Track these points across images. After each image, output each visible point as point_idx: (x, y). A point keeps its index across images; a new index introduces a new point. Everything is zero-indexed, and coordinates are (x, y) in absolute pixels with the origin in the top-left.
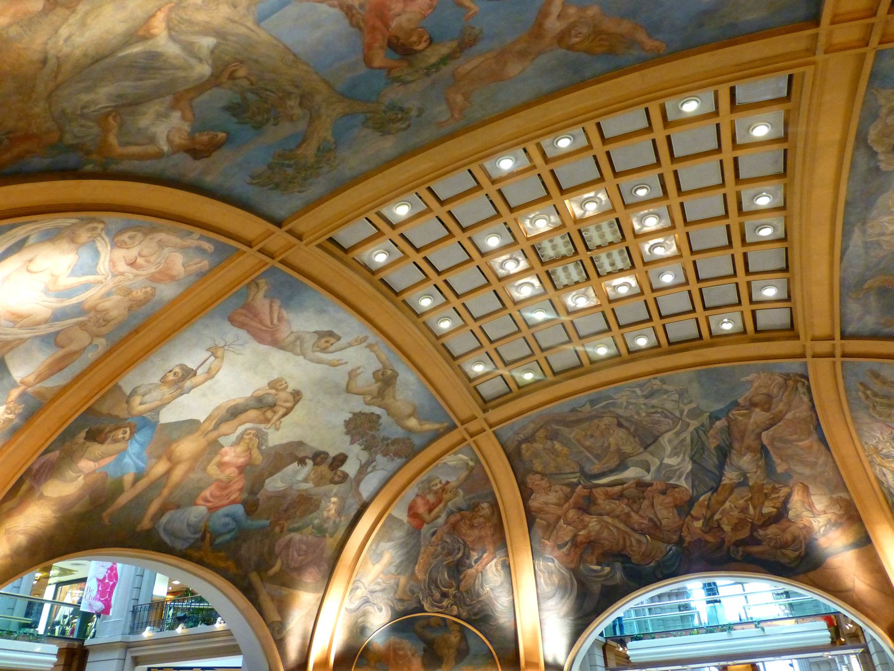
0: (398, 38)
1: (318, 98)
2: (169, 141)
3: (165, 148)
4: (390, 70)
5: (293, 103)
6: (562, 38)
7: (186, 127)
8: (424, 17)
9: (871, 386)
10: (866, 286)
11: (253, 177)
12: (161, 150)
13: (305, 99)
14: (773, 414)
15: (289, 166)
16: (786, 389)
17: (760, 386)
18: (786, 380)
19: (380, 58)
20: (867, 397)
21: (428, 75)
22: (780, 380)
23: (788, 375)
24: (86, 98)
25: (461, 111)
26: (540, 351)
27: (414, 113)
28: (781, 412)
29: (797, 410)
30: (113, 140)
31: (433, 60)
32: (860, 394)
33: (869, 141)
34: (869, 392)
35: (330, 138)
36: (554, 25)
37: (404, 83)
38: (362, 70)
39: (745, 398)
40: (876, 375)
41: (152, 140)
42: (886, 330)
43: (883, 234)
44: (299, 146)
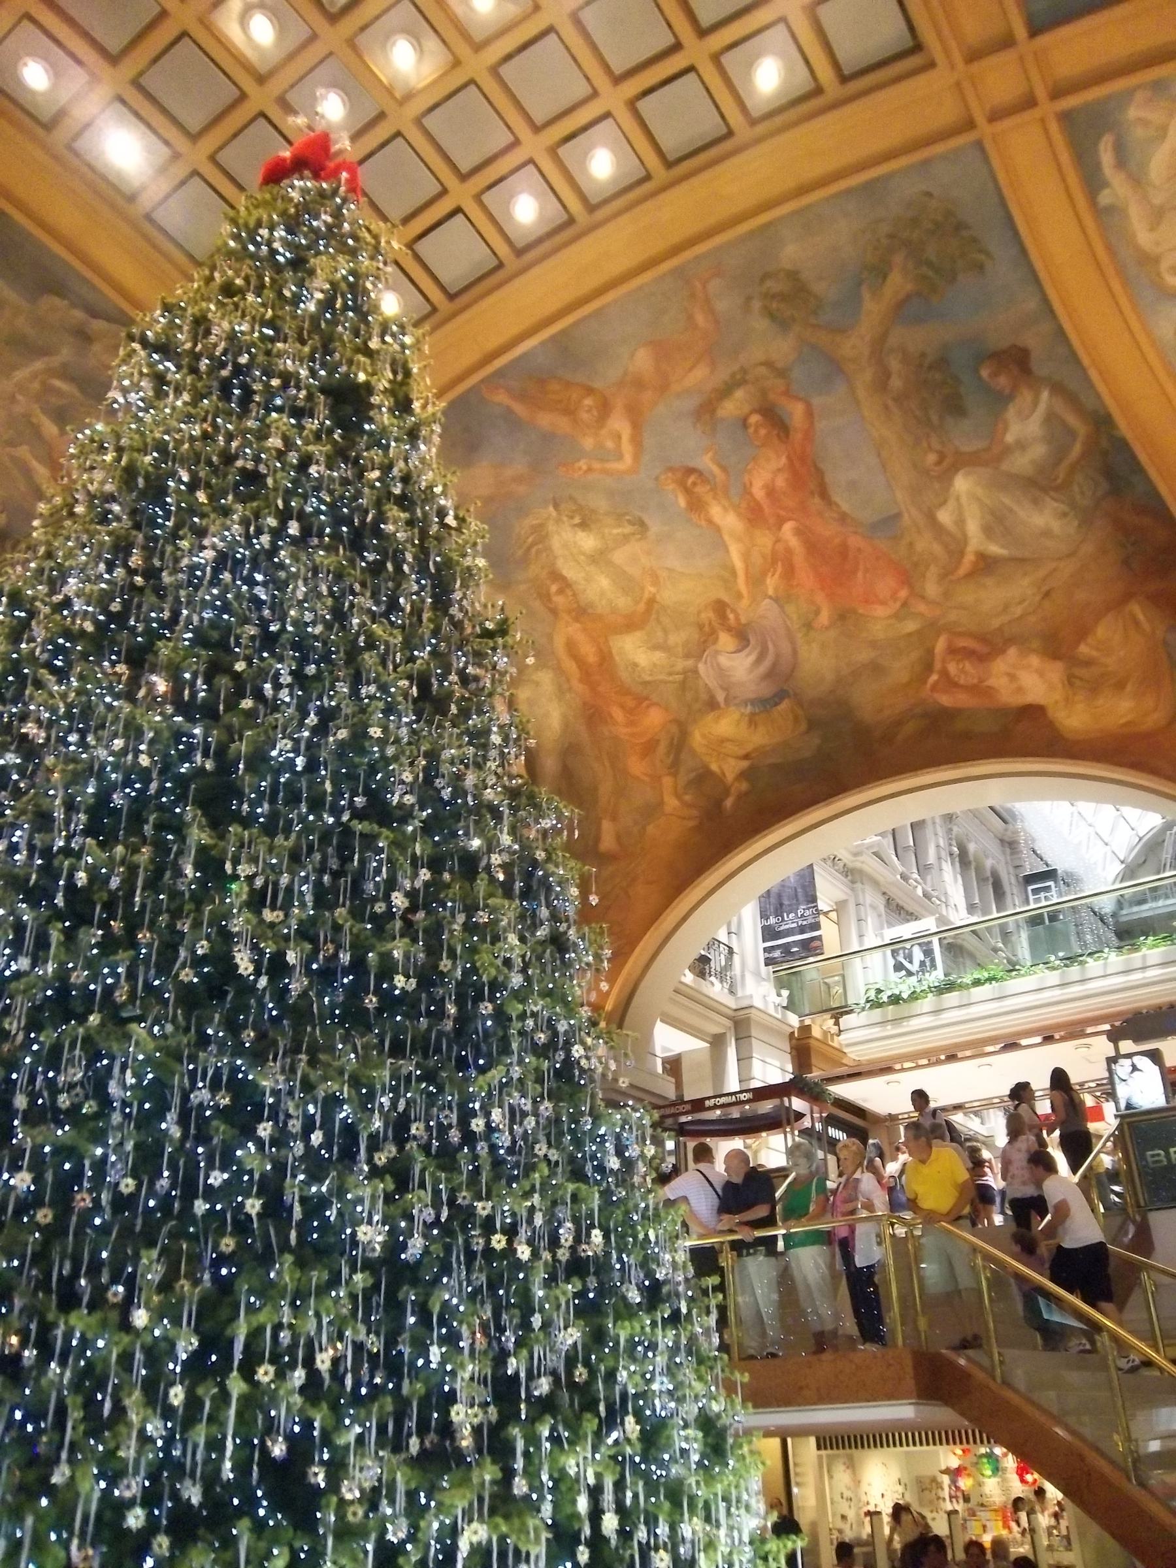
0: (778, 436)
1: (868, 375)
2: (1035, 404)
3: (1045, 395)
4: (787, 393)
5: (896, 383)
6: (605, 409)
7: (1011, 413)
8: (754, 459)
11: (981, 267)
12: (1051, 395)
13: (881, 383)
15: (929, 264)
19: (796, 413)
21: (744, 371)
24: (1056, 526)
25: (693, 296)
26: (478, 80)
27: (757, 305)
30: (1077, 449)
31: (739, 394)
35: (866, 295)
36: (619, 424)
37: (768, 364)
38: (817, 401)
41: (1051, 418)
44: (908, 297)
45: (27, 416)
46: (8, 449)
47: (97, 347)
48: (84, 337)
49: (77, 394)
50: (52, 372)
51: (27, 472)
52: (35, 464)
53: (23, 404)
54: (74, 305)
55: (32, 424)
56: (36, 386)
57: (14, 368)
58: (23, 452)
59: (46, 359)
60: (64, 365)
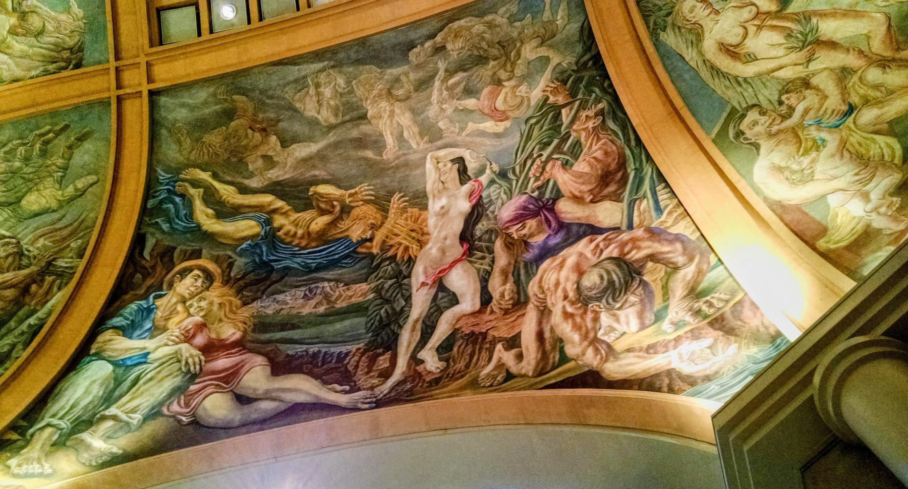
9: (62, 137)
10: (235, 97)
14: (6, 39)
16: (52, 50)
17: (59, 22)
18: (71, 49)
20: (43, 135)
22: (71, 42)
23: (81, 49)
28: (8, 47)
29: (13, 66)
32: (48, 127)
33: (450, 25)
34: (51, 135)
39: (36, 6)
40: (81, 139)
42: (164, 132)
43: (317, 86)
45: (456, 110)
46: (464, 134)
47: (449, 46)
48: (440, 49)
49: (465, 74)
50: (445, 80)
51: (483, 134)
52: (482, 126)
53: (449, 108)
54: (422, 44)
55: (462, 110)
56: (445, 93)
57: (430, 97)
58: (471, 126)
59: (437, 77)
60: (446, 71)
